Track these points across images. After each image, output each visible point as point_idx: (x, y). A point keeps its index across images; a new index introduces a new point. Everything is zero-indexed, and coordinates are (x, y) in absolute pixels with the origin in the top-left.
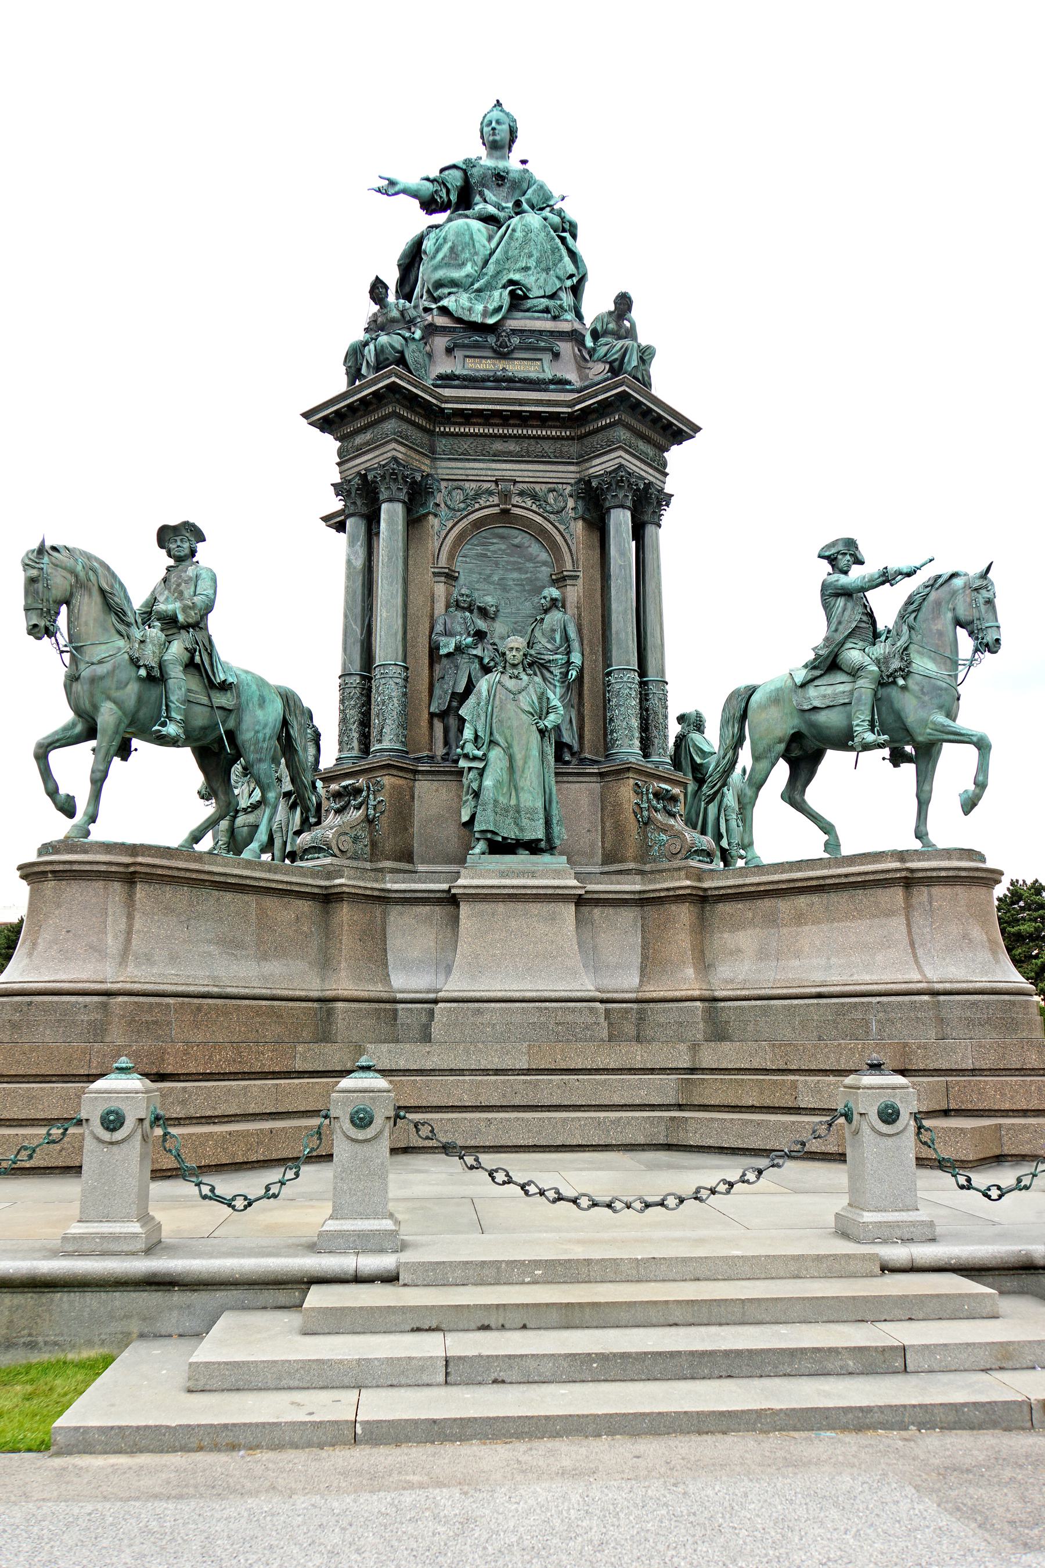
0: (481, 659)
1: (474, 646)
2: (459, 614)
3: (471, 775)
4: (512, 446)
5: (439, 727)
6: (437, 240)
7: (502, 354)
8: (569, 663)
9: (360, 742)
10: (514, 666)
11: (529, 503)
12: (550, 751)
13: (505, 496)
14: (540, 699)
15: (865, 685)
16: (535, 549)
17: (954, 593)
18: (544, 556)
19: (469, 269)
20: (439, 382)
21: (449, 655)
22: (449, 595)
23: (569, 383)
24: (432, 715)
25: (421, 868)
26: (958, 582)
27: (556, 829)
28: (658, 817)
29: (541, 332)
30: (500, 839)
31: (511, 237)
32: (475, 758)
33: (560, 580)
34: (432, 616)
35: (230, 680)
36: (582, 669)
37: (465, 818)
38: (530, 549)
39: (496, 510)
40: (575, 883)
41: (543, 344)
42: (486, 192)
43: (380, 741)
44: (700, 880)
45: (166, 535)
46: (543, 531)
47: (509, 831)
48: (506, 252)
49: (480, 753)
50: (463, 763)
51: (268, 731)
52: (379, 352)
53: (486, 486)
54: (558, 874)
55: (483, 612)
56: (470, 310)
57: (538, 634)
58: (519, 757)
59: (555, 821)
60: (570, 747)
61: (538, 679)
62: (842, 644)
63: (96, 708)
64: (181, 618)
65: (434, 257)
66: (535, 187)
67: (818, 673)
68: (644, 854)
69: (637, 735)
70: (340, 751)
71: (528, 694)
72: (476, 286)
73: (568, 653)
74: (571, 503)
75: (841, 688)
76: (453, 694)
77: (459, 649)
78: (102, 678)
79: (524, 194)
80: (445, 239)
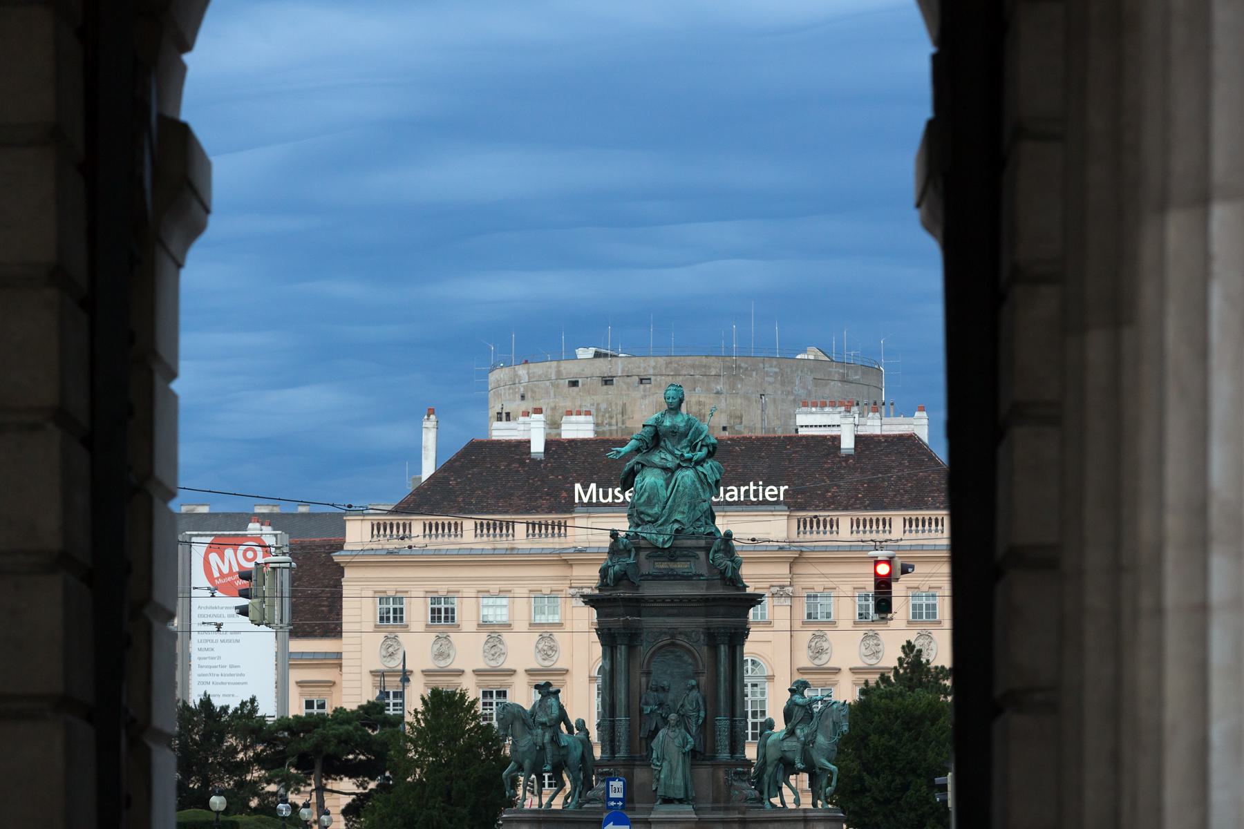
0: (661, 715)
1: (658, 709)
2: (652, 693)
3: (656, 772)
4: (675, 611)
5: (644, 743)
6: (642, 487)
7: (672, 558)
8: (699, 716)
9: (610, 750)
10: (673, 727)
11: (683, 637)
12: (688, 760)
13: (673, 636)
14: (683, 740)
15: (799, 746)
16: (686, 658)
17: (833, 711)
18: (690, 661)
19: (656, 510)
20: (642, 578)
21: (647, 714)
22: (648, 683)
23: (702, 575)
24: (641, 738)
25: (638, 806)
26: (835, 706)
27: (690, 793)
28: (735, 783)
29: (690, 548)
30: (667, 798)
31: (677, 491)
32: (657, 765)
33: (697, 674)
34: (640, 693)
35: (566, 745)
36: (705, 720)
37: (654, 789)
38: (685, 658)
39: (669, 642)
40: (695, 816)
41: (690, 554)
42: (667, 440)
43: (619, 752)
44: (744, 813)
45: (537, 687)
46: (690, 651)
47: (671, 795)
48: (674, 500)
49: (659, 764)
50: (652, 766)
51: (578, 759)
52: (615, 574)
53: (664, 630)
54: (688, 813)
55: (663, 689)
56: (657, 540)
57: (686, 702)
58: (675, 765)
59: (689, 790)
60: (700, 752)
61: (683, 730)
62: (796, 726)
63: (523, 762)
64: (548, 724)
65: (639, 499)
66: (693, 429)
67: (787, 736)
68: (728, 799)
69: (728, 747)
70: (602, 753)
71: (679, 739)
72: (660, 522)
73: (699, 711)
74: (702, 637)
75: (794, 744)
76: (650, 731)
77: (651, 711)
78: (526, 752)
79: (686, 436)
80: (645, 489)
